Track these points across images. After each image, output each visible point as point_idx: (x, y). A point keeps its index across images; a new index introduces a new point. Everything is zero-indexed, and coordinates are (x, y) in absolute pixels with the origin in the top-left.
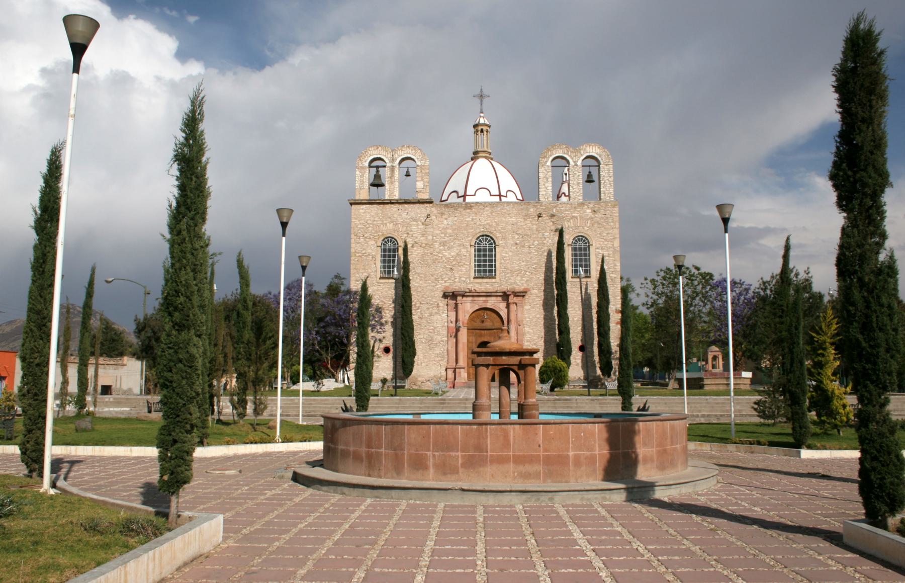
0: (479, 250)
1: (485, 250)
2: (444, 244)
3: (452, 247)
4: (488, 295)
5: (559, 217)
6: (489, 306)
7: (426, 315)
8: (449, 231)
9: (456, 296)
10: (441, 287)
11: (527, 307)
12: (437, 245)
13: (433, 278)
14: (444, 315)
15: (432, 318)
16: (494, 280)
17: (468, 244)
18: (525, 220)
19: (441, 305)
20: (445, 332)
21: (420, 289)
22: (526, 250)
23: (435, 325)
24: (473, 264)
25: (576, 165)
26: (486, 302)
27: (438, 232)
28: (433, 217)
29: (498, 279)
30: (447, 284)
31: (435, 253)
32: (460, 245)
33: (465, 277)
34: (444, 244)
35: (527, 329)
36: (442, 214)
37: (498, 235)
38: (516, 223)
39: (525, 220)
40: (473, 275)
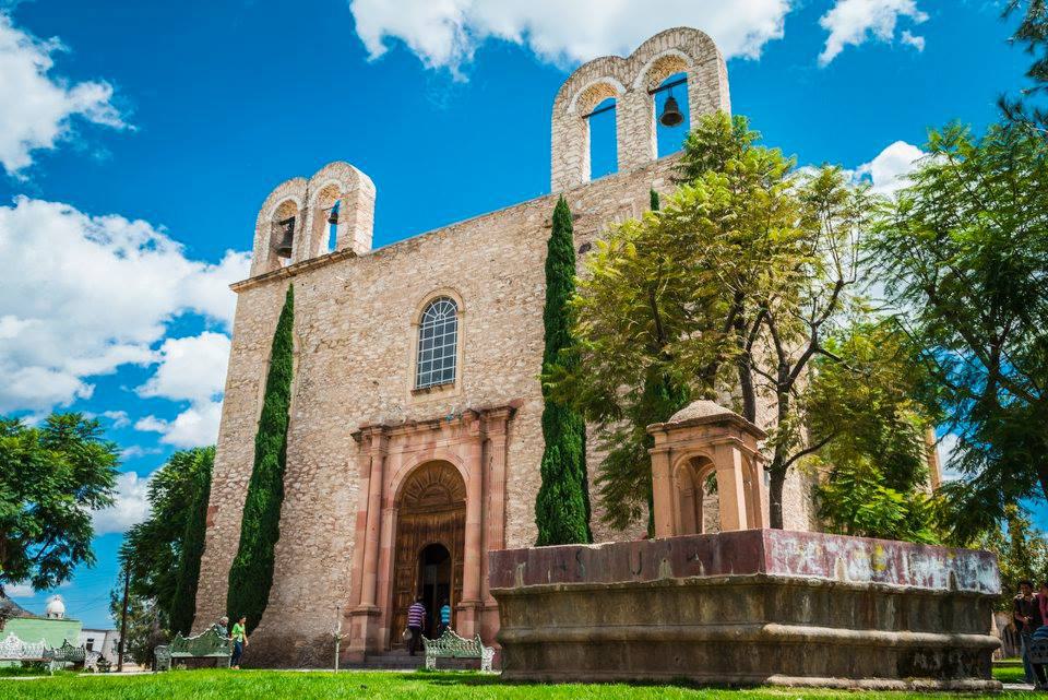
0: (429, 333)
1: (440, 331)
2: (364, 334)
3: (381, 335)
4: (435, 425)
5: (589, 217)
6: (438, 455)
7: (324, 492)
8: (378, 305)
9: (369, 439)
10: (354, 426)
11: (515, 447)
12: (355, 338)
13: (343, 410)
14: (354, 488)
15: (334, 497)
16: (450, 393)
17: (407, 324)
18: (517, 243)
19: (351, 465)
20: (352, 528)
21: (319, 437)
22: (517, 310)
23: (337, 514)
24: (413, 366)
25: (631, 90)
26: (432, 445)
27: (358, 312)
28: (354, 284)
29: (458, 388)
30: (365, 418)
31: (351, 356)
32: (394, 330)
33: (398, 397)
34: (364, 334)
35: (514, 503)
36: (370, 272)
37: (464, 290)
38: (500, 255)
39: (517, 243)
40: (411, 385)
